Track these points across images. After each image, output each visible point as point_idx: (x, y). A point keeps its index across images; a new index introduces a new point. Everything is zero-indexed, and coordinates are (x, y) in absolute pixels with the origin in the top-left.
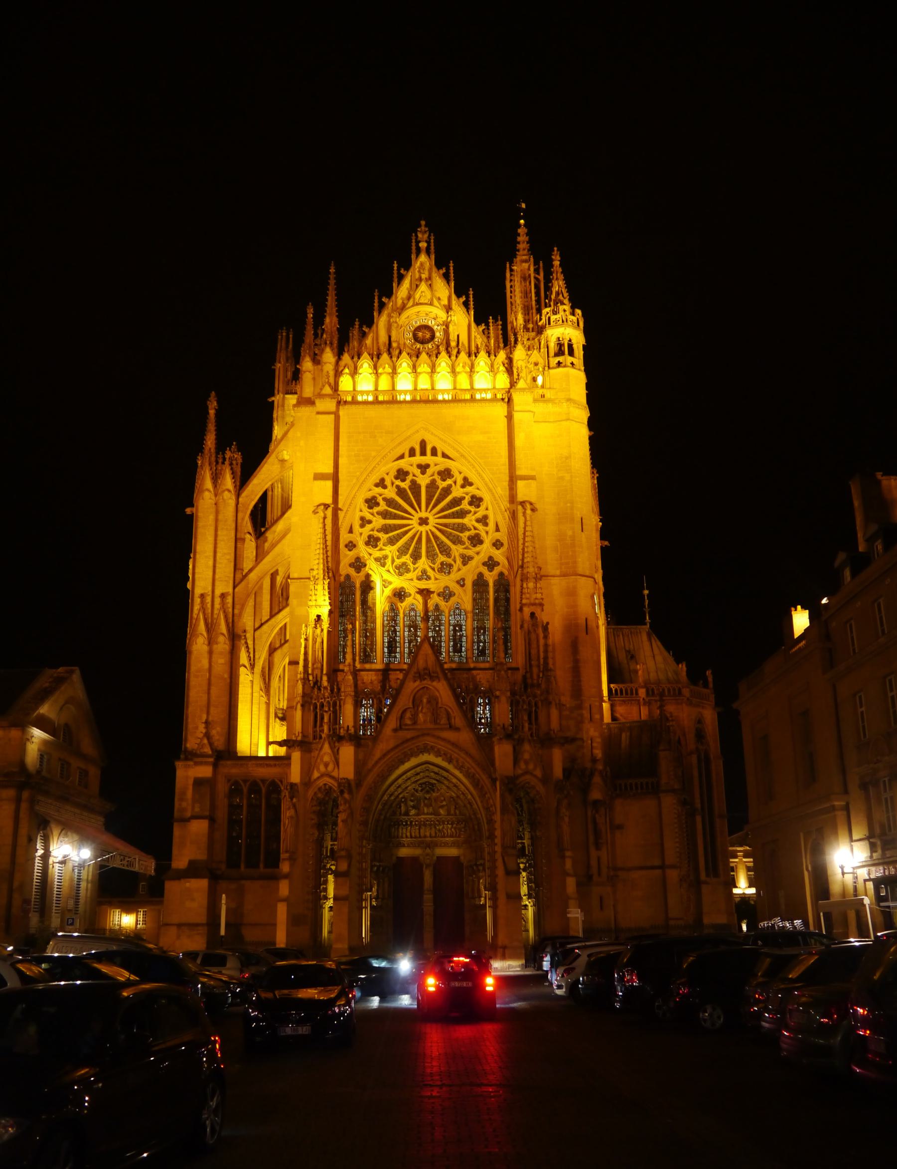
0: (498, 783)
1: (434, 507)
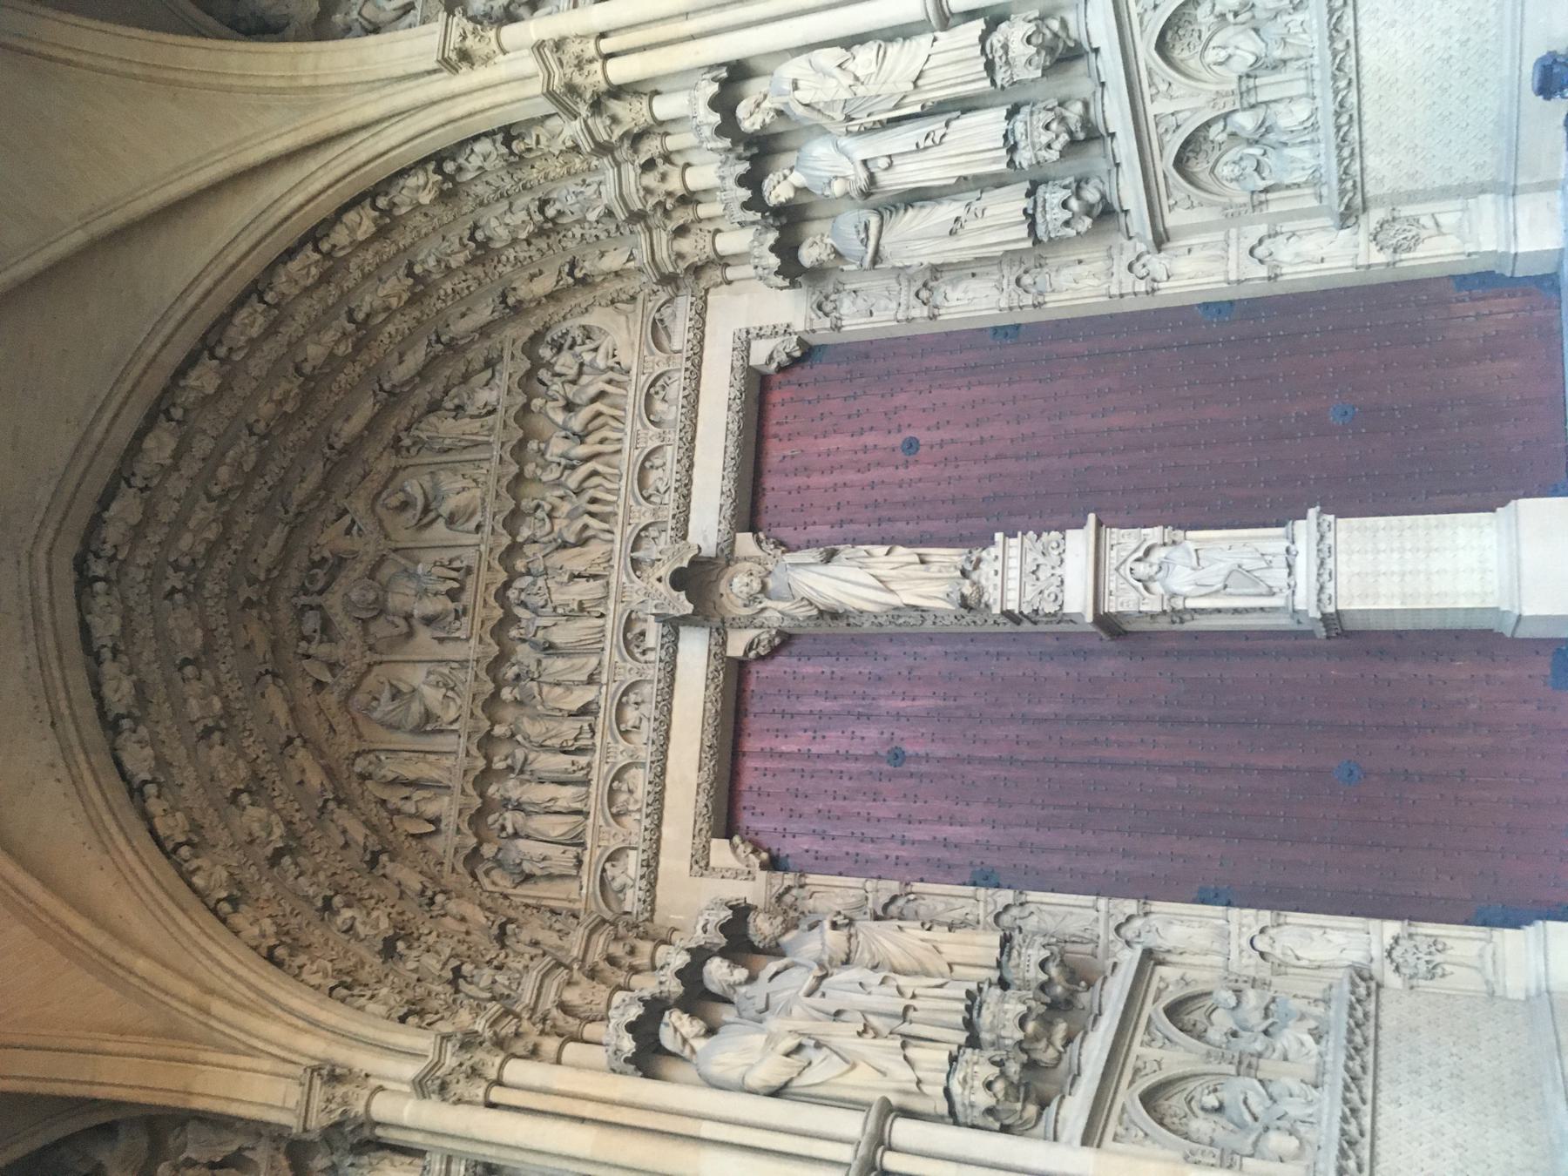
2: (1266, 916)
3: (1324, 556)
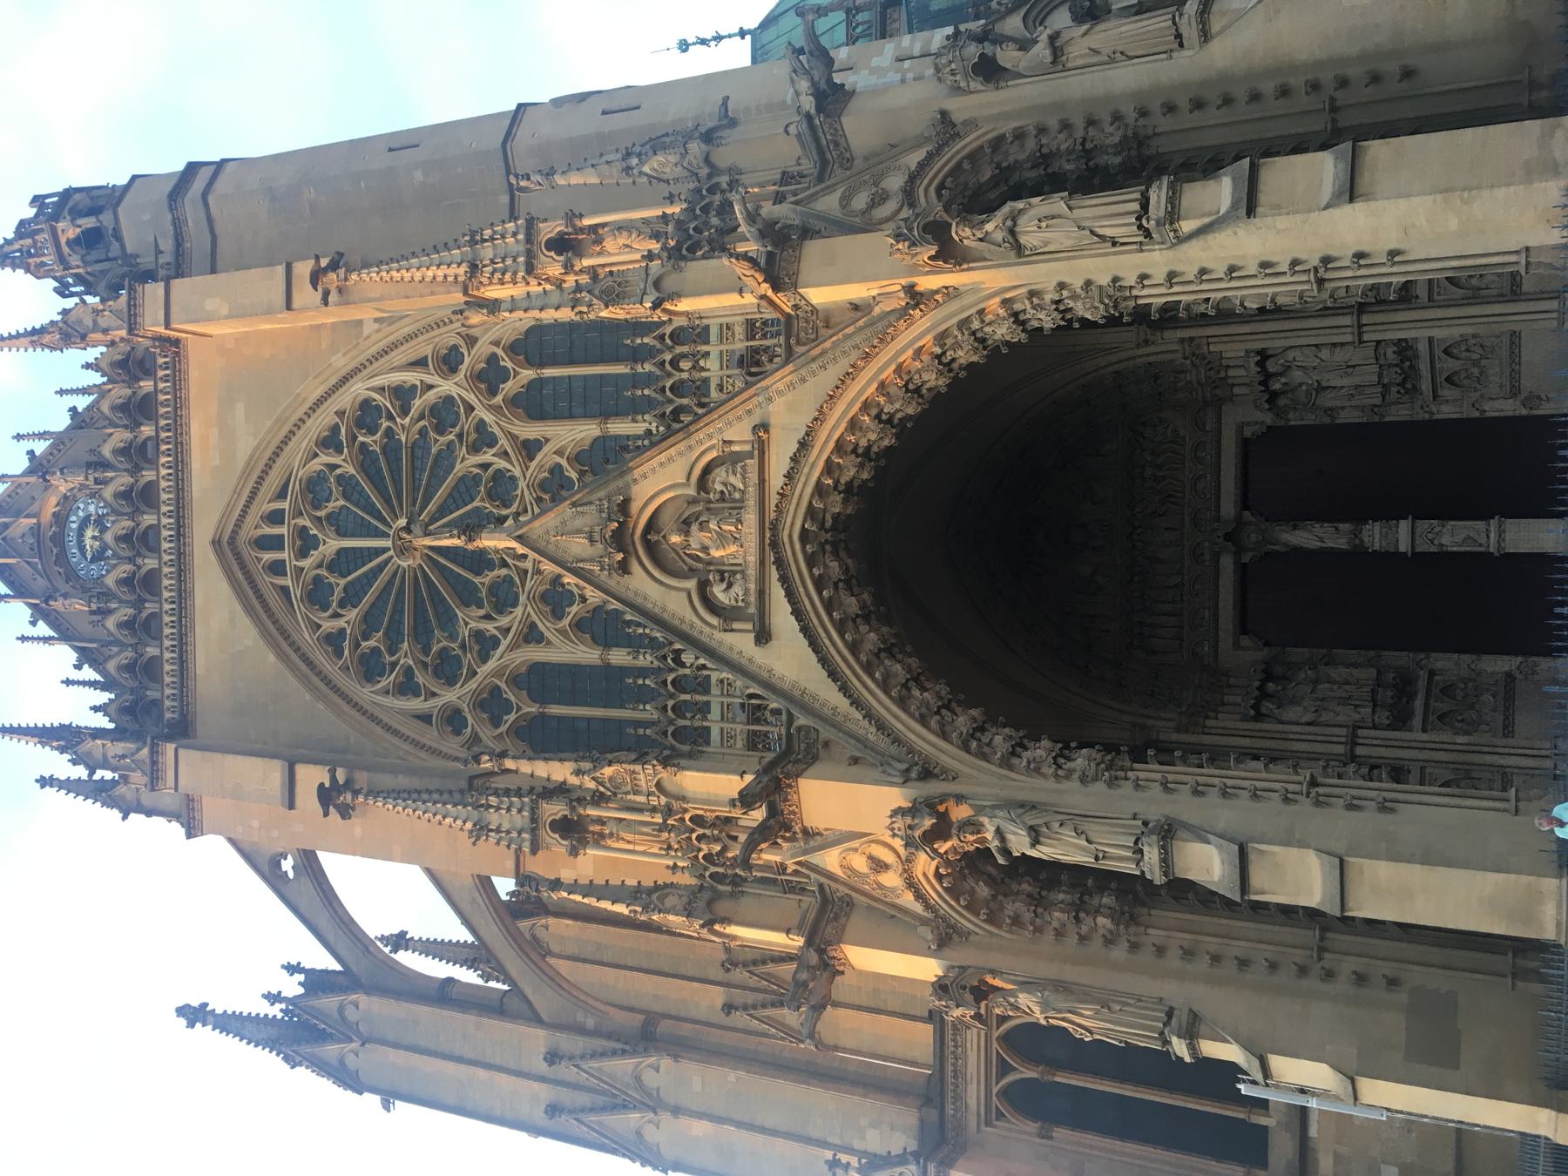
0: (927, 283)
2: (1474, 657)
3: (1501, 532)
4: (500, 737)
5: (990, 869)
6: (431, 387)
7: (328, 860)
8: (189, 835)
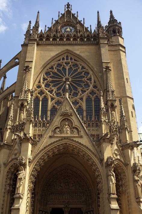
1: (70, 76)
4: (36, 94)
5: (15, 171)
6: (91, 84)
7: (18, 66)
8: (22, 45)
